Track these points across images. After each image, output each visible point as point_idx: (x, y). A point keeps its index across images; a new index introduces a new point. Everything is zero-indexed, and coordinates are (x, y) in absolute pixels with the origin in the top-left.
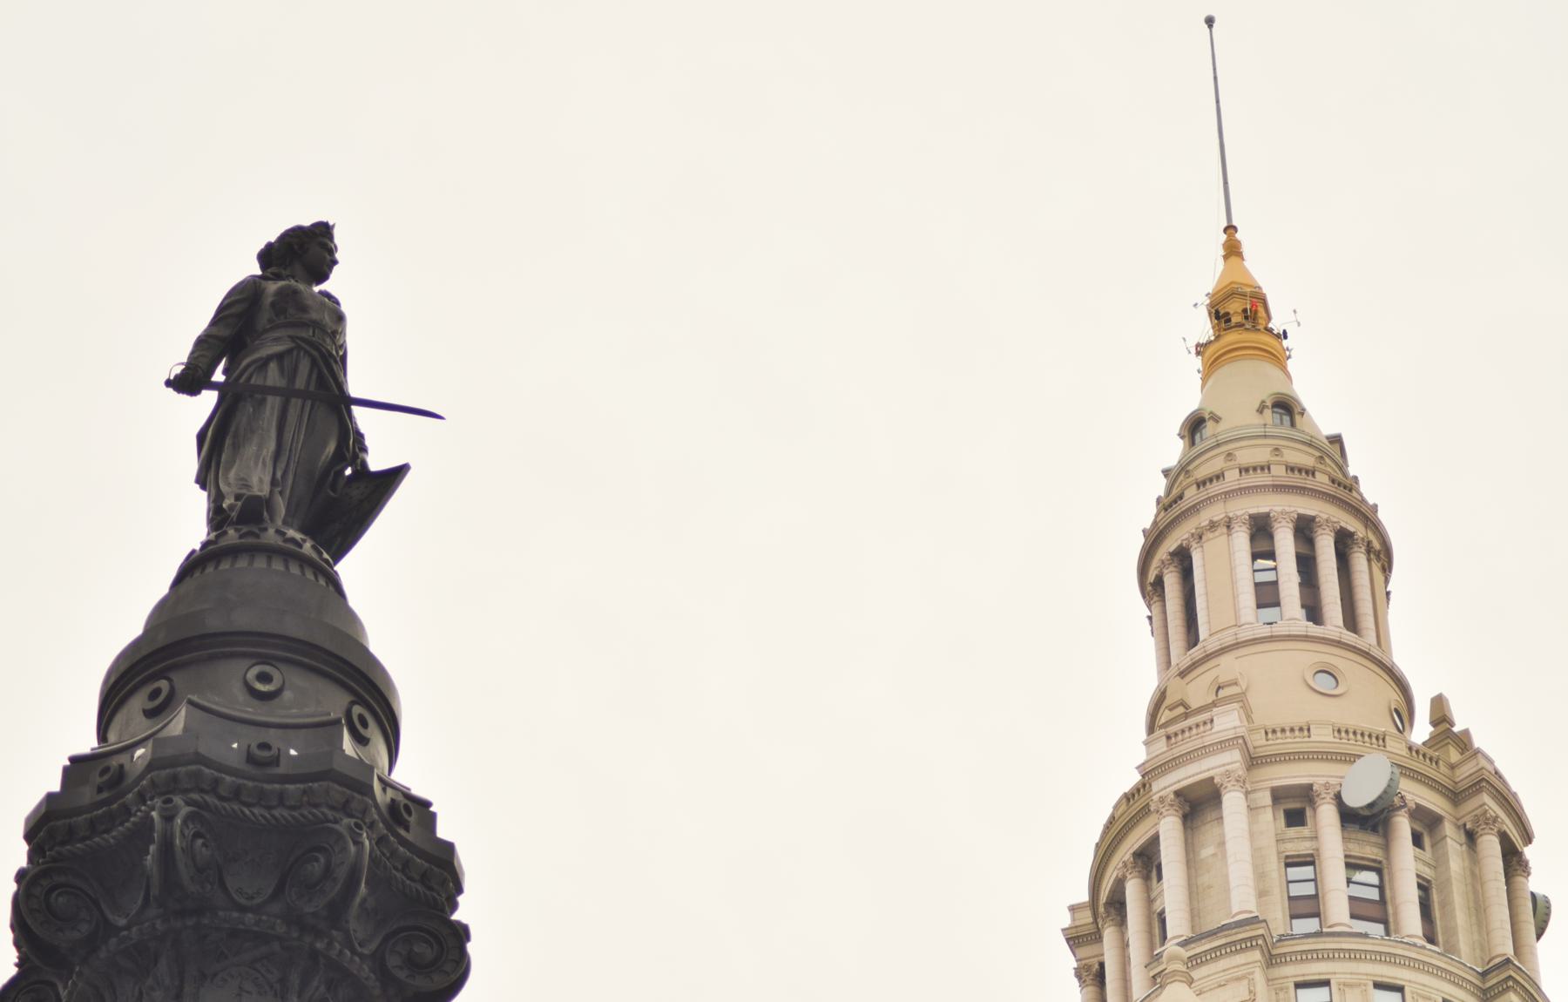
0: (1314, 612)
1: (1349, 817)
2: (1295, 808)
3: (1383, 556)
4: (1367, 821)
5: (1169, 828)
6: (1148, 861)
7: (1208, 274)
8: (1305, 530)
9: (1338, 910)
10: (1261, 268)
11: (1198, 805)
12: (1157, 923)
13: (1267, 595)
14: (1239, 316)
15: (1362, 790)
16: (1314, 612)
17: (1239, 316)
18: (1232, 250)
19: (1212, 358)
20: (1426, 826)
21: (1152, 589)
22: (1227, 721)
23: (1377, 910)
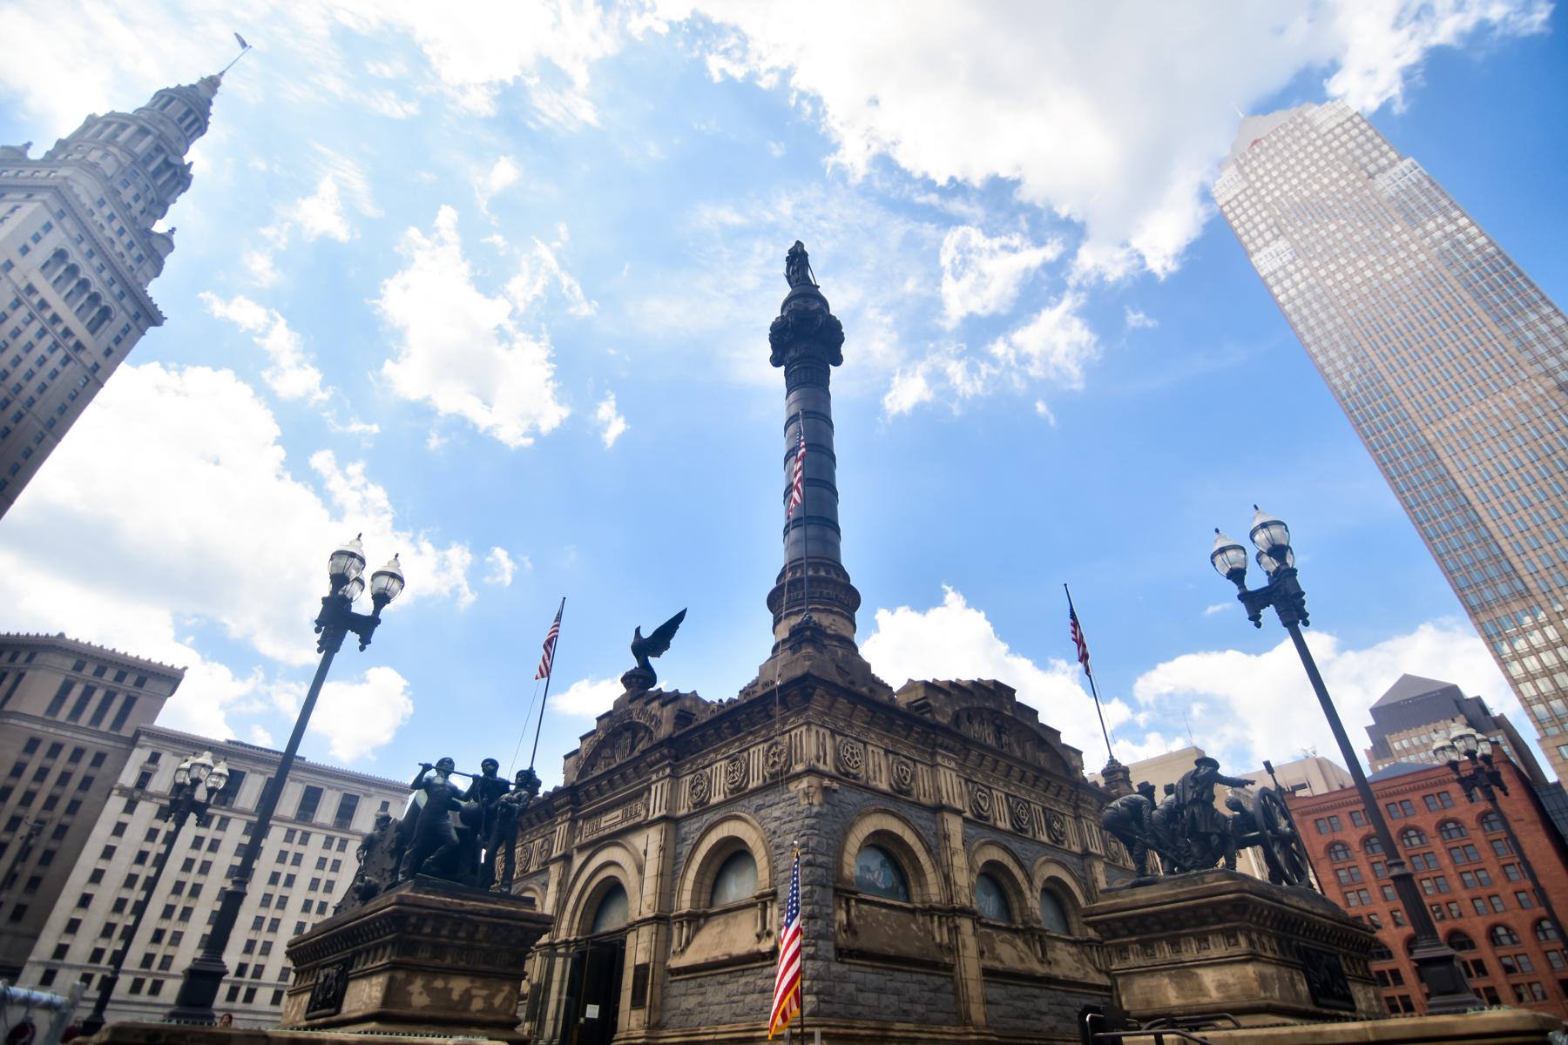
0: (187, 128)
2: (159, 149)
4: (167, 164)
6: (123, 127)
7: (215, 73)
9: (152, 168)
10: (223, 80)
11: (144, 131)
15: (173, 159)
16: (187, 128)
18: (222, 74)
19: (203, 81)
20: (175, 174)
22: (162, 128)
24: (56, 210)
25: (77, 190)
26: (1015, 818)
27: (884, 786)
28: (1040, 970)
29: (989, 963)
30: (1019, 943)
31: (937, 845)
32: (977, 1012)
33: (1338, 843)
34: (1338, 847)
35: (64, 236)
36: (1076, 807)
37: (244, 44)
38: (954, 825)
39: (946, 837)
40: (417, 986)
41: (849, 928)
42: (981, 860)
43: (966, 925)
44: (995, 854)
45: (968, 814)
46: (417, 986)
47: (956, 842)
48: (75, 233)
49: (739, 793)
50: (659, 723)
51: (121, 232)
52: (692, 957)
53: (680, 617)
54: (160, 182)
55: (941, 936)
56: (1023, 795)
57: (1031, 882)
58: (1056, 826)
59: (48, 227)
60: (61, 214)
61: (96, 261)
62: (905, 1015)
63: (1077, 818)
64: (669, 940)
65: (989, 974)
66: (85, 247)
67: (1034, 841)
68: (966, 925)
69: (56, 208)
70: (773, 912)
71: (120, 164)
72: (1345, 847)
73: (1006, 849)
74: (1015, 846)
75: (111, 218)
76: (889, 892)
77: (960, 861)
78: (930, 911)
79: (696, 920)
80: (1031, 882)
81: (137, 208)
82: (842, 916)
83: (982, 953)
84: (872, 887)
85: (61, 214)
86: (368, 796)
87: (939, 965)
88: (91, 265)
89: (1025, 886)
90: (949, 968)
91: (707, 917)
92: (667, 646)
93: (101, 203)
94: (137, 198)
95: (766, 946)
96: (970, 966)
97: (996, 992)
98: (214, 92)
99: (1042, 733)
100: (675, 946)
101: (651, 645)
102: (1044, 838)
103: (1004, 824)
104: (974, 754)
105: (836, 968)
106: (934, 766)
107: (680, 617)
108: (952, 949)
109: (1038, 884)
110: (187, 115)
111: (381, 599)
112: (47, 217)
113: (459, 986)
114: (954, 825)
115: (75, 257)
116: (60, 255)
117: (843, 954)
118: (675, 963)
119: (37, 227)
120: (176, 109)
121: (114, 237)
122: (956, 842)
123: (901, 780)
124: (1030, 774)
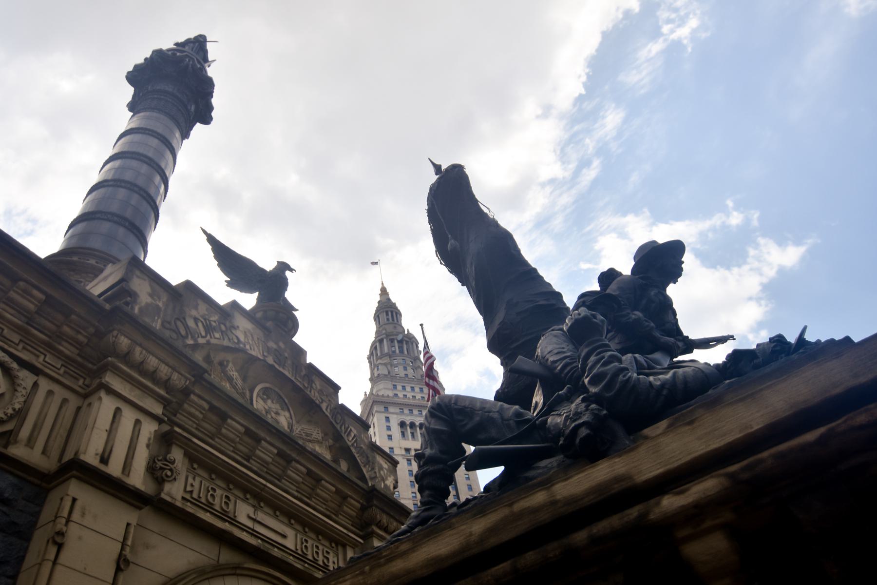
1: (398, 342)
2: (392, 341)
3: (401, 315)
5: (378, 344)
8: (392, 312)
9: (397, 351)
10: (385, 285)
12: (377, 355)
13: (388, 319)
14: (384, 292)
15: (400, 337)
17: (384, 292)
19: (381, 295)
20: (407, 343)
21: (375, 320)
23: (401, 351)
24: (383, 409)
25: (380, 393)
35: (395, 416)
37: (376, 263)
48: (398, 411)
51: (413, 389)
54: (406, 352)
59: (387, 419)
60: (386, 408)
61: (416, 412)
66: (406, 411)
69: (382, 408)
71: (385, 364)
75: (404, 388)
81: (410, 372)
85: (386, 408)
88: (416, 416)
93: (395, 387)
94: (405, 369)
98: (387, 294)
110: (387, 315)
112: (383, 416)
115: (408, 420)
116: (402, 424)
119: (384, 423)
120: (383, 317)
121: (413, 394)
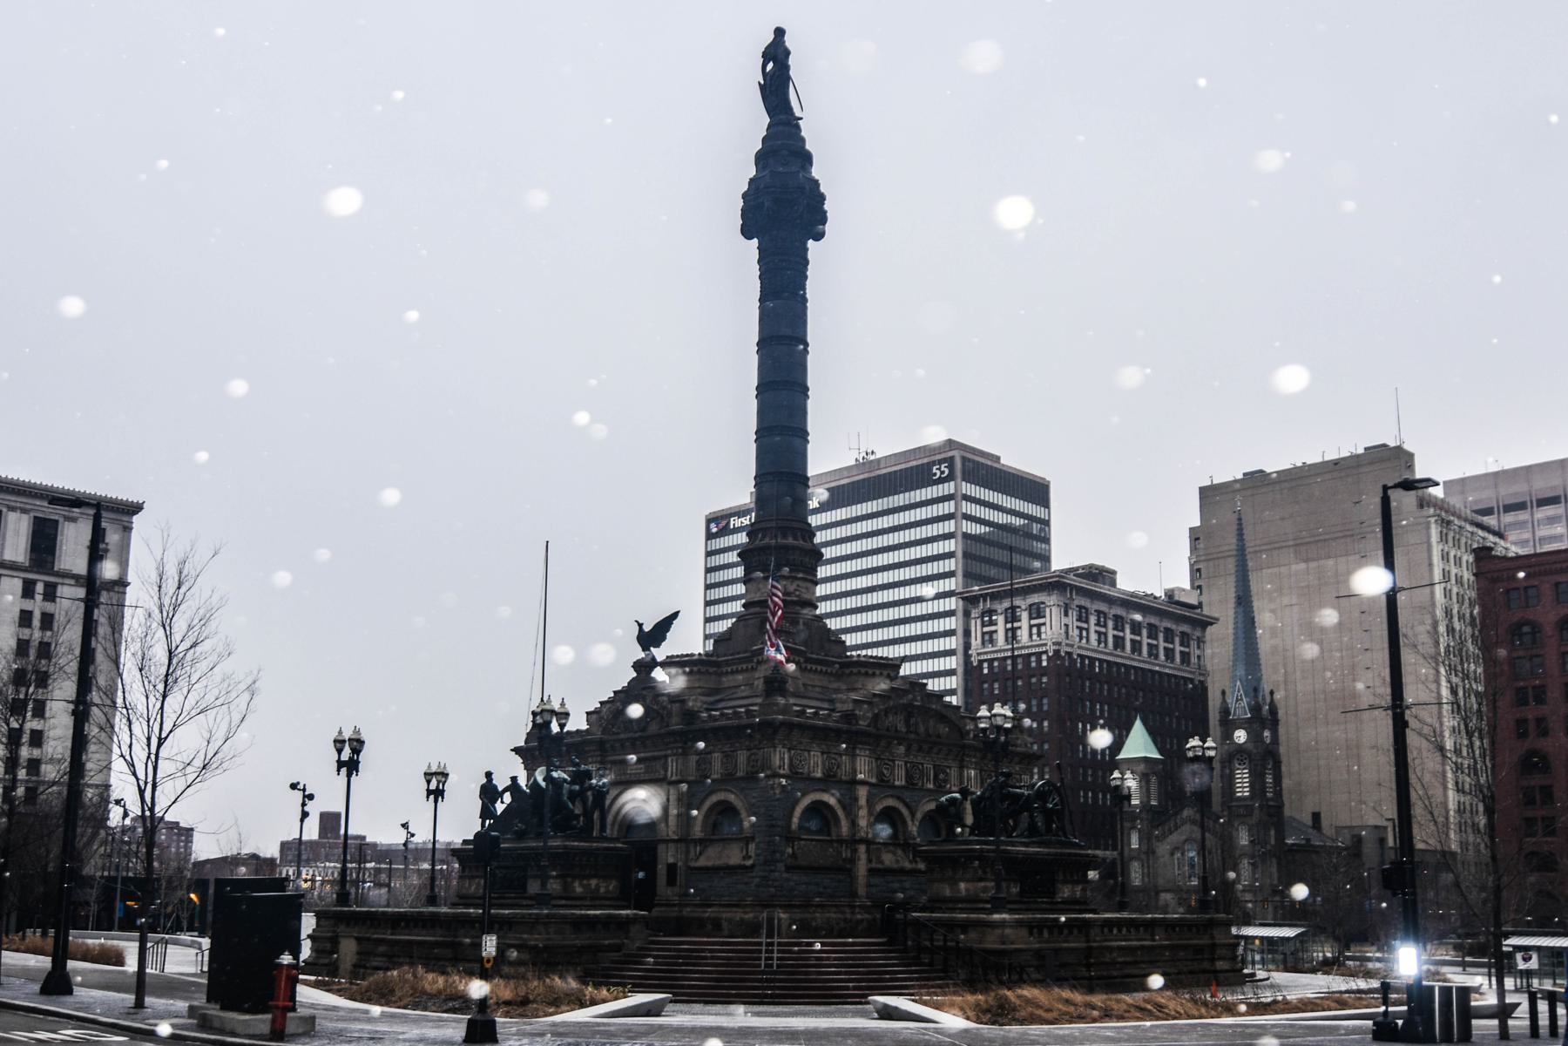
26: (909, 777)
27: (819, 774)
28: (907, 865)
29: (874, 865)
30: (899, 852)
31: (849, 805)
32: (862, 891)
33: (1527, 623)
34: (1526, 629)
36: (962, 760)
38: (862, 792)
39: (856, 799)
40: (576, 884)
41: (794, 855)
42: (879, 808)
43: (862, 848)
44: (890, 802)
45: (874, 780)
46: (576, 884)
47: (863, 801)
49: (728, 779)
50: (670, 714)
52: (702, 862)
53: (675, 615)
55: (846, 853)
56: (920, 759)
57: (913, 815)
58: (942, 776)
62: (820, 895)
63: (961, 768)
64: (688, 852)
65: (872, 872)
67: (921, 789)
68: (862, 848)
70: (752, 846)
72: (1536, 628)
73: (899, 798)
74: (906, 795)
76: (819, 832)
77: (863, 812)
78: (841, 841)
79: (704, 843)
80: (913, 815)
82: (790, 850)
83: (870, 861)
84: (809, 831)
86: (74, 520)
87: (845, 869)
89: (909, 819)
90: (850, 870)
91: (711, 841)
92: (664, 638)
95: (749, 863)
96: (862, 868)
97: (876, 880)
99: (944, 711)
100: (692, 854)
101: (652, 637)
102: (931, 786)
103: (900, 782)
104: (883, 743)
105: (785, 875)
106: (853, 756)
107: (675, 615)
108: (853, 861)
109: (919, 815)
111: (562, 726)
113: (594, 882)
114: (862, 792)
117: (789, 869)
118: (693, 864)
122: (863, 801)
123: (830, 769)
124: (925, 747)
